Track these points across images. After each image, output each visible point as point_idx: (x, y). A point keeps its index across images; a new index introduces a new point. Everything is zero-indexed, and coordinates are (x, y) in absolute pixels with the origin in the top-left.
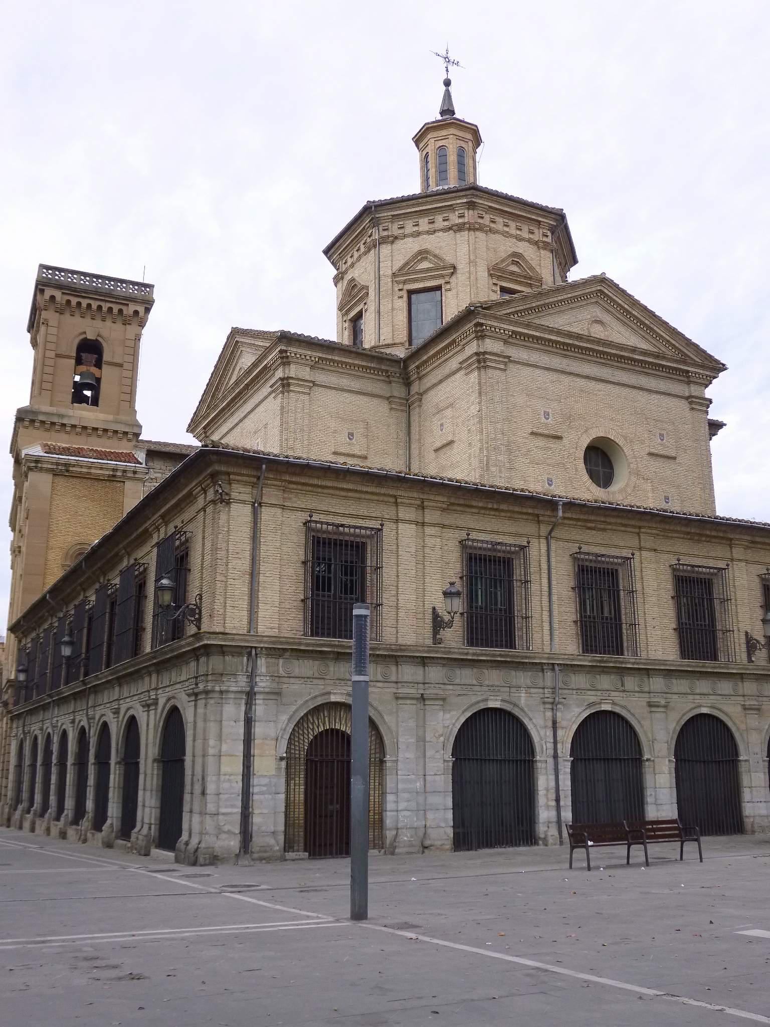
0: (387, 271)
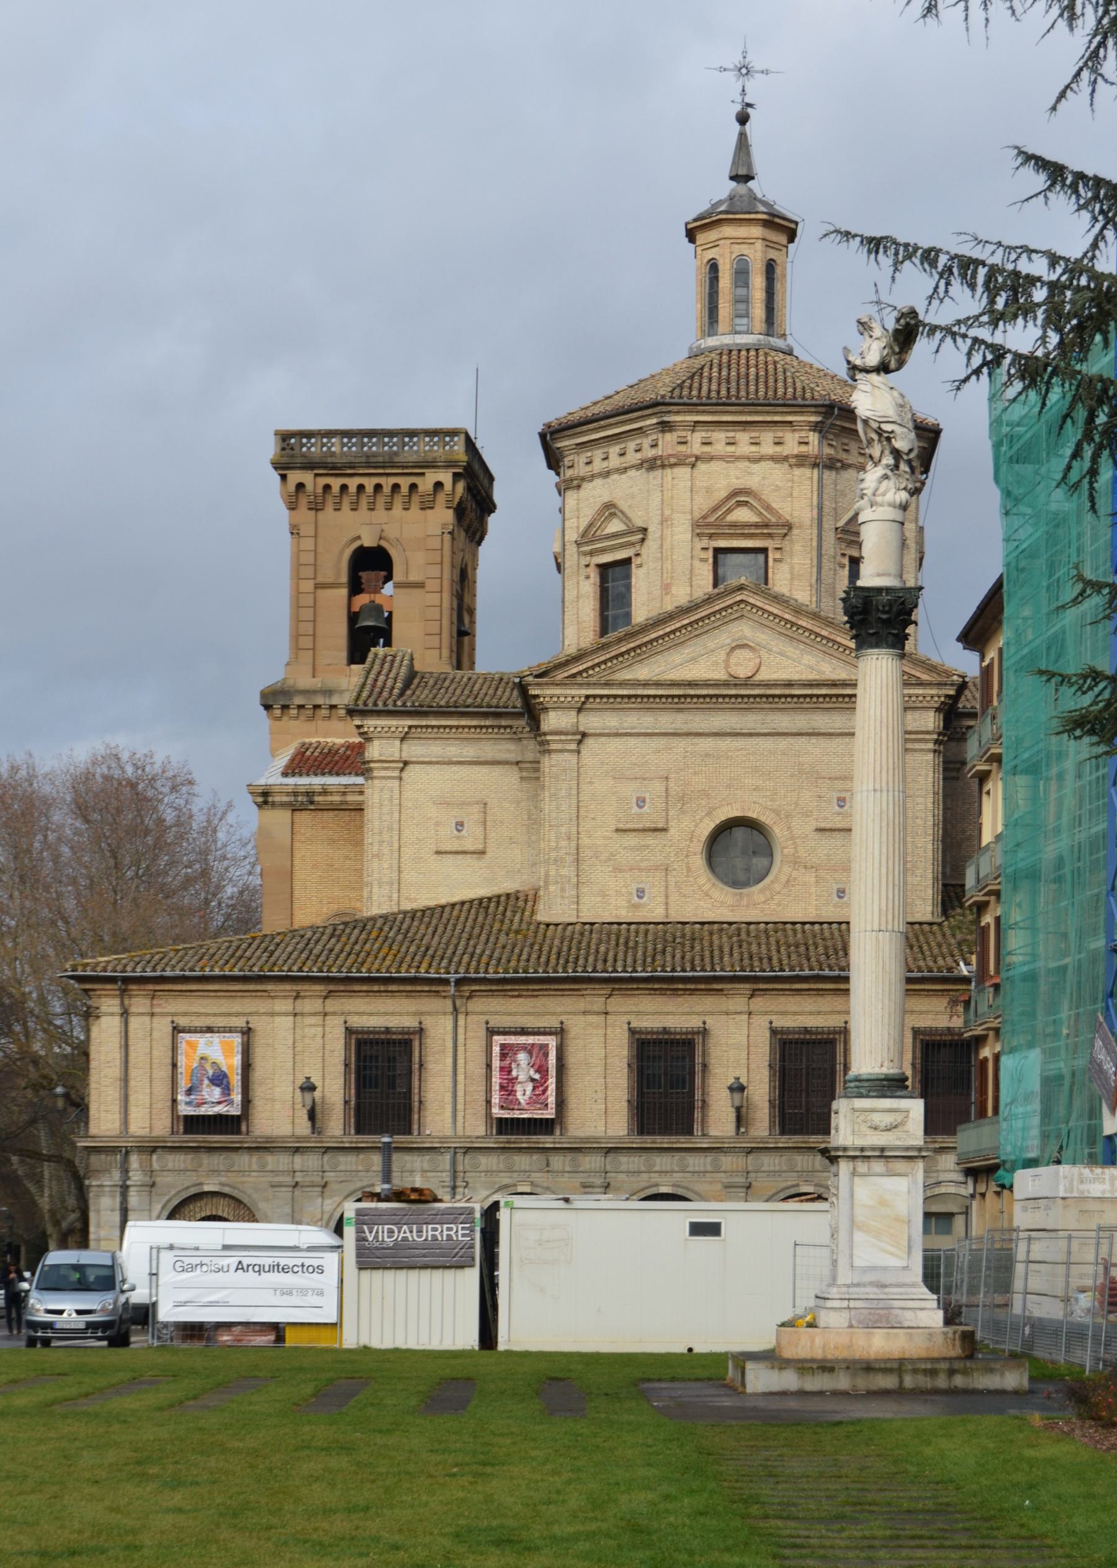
0: (572, 536)
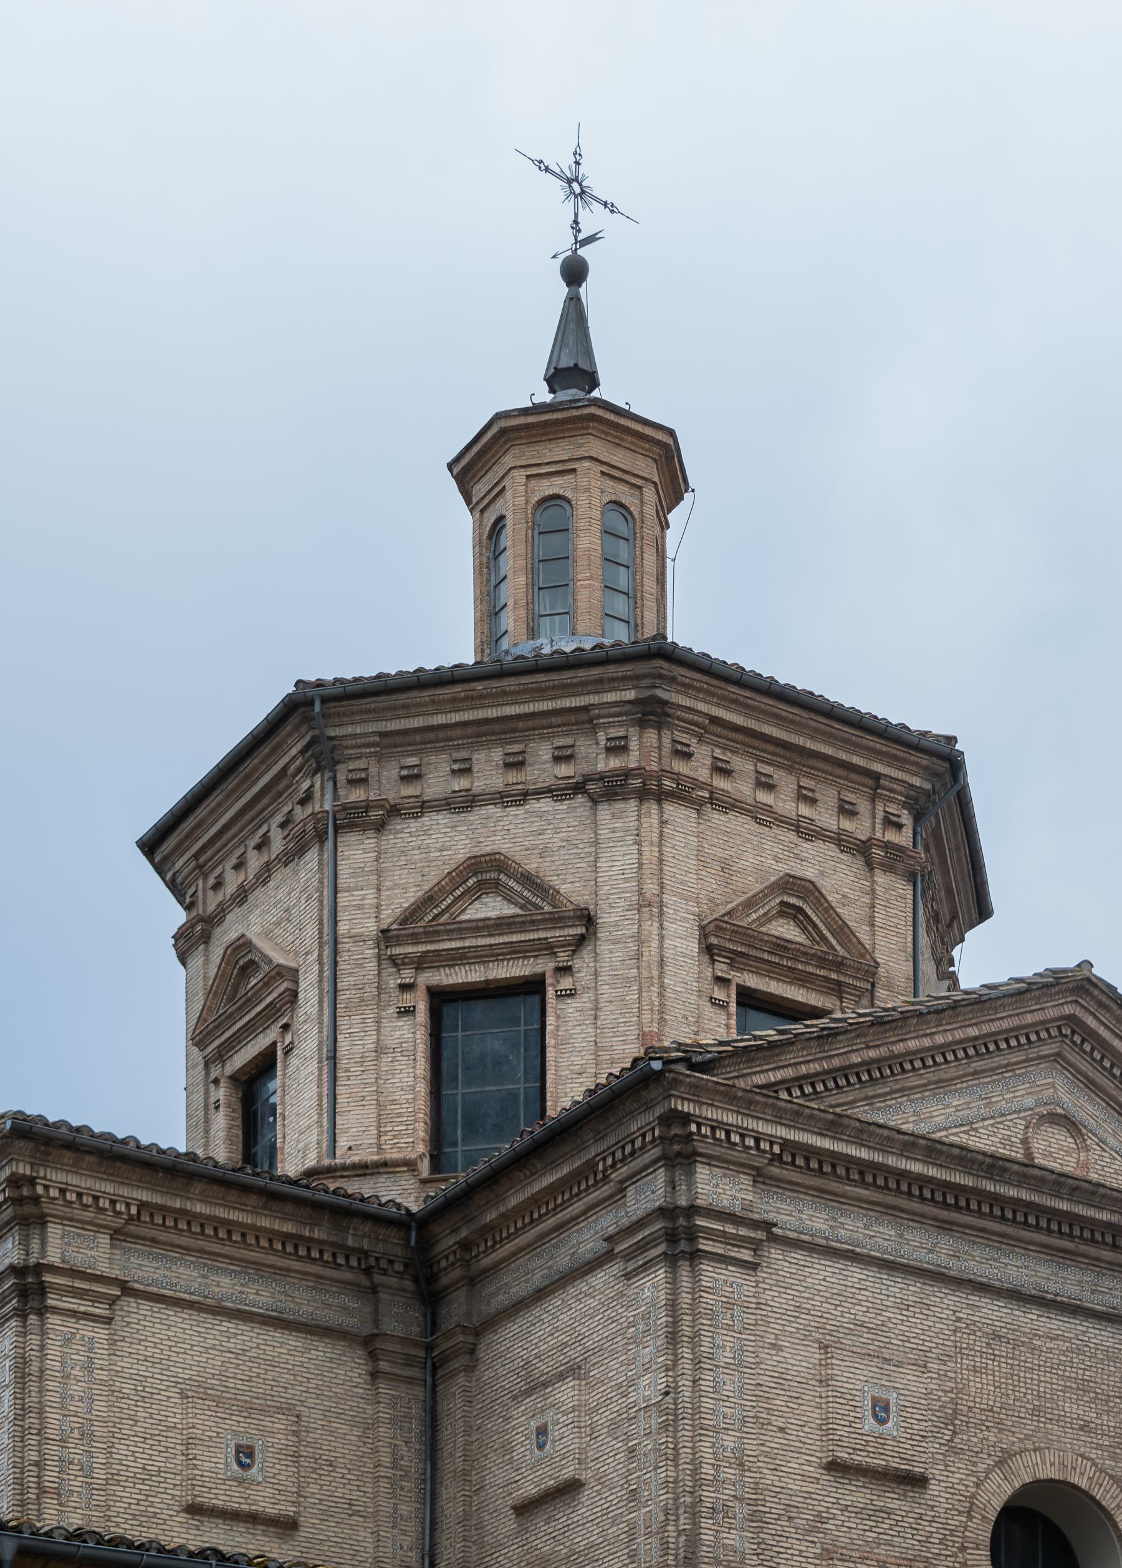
0: (360, 921)
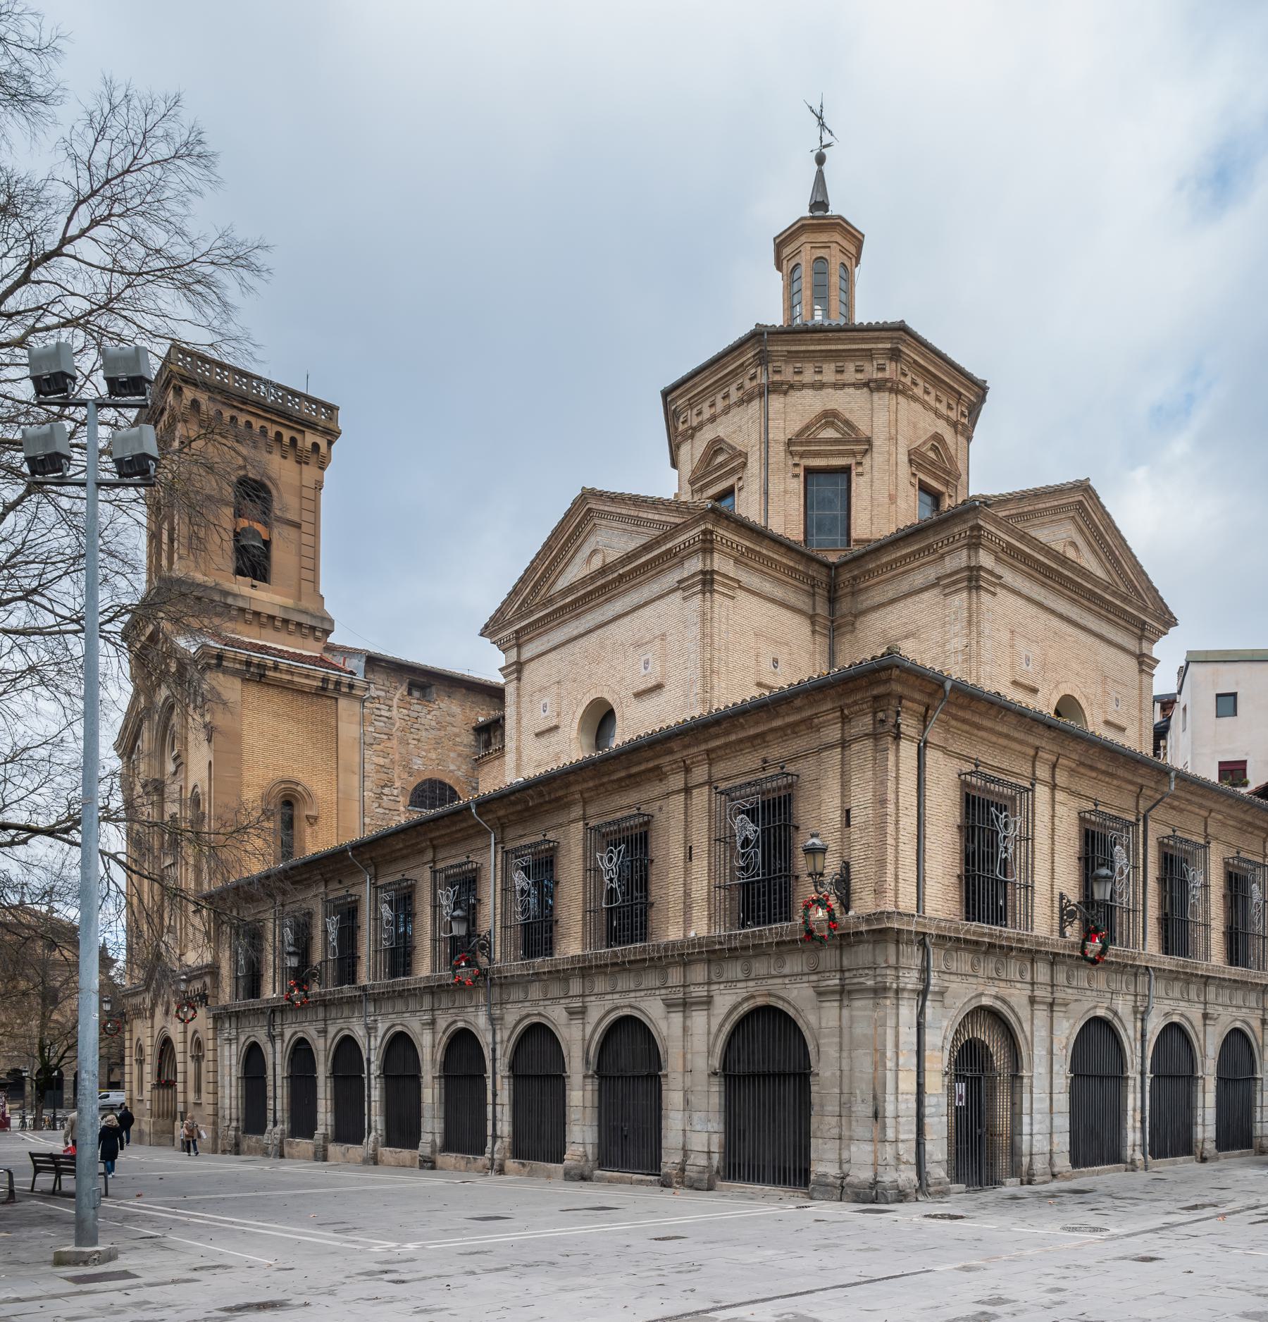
0: (779, 434)
